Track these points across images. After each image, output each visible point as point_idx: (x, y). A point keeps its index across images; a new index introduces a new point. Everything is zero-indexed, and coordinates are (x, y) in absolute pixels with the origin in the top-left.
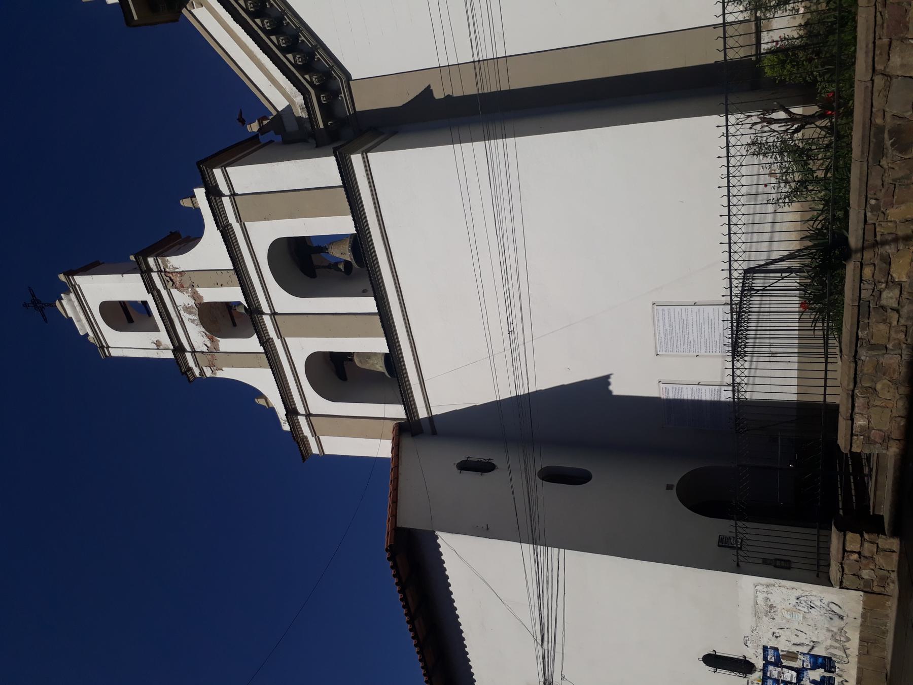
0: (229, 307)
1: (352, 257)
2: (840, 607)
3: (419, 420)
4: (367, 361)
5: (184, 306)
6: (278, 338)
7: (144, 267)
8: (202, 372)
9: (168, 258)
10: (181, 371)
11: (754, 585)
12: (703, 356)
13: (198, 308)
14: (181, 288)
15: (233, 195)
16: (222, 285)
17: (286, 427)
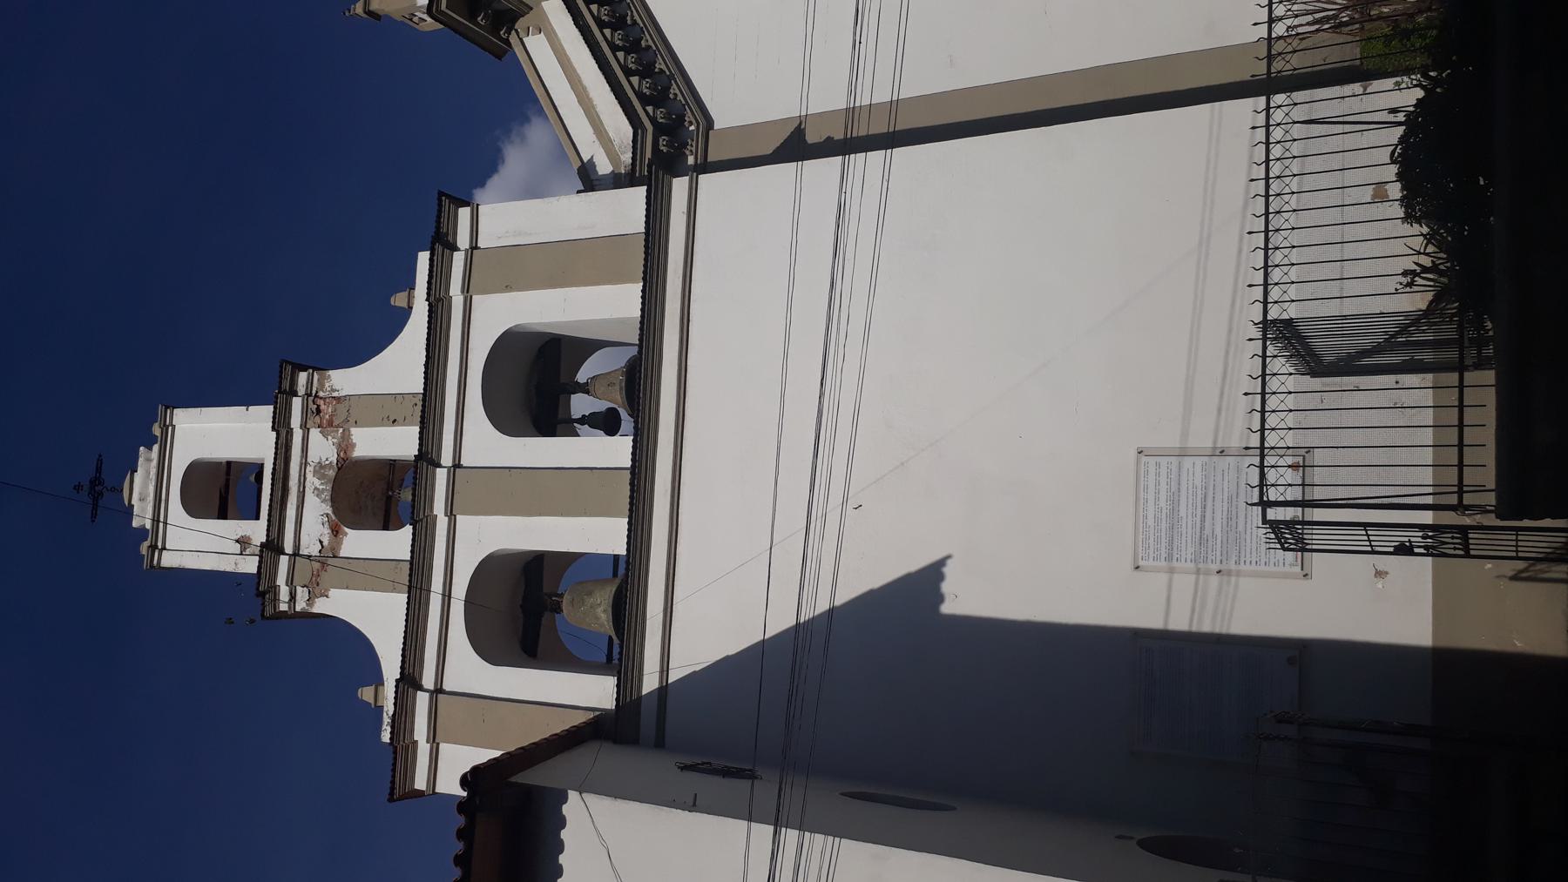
0: (391, 468)
1: (623, 384)
5: (319, 463)
6: (446, 515)
7: (286, 385)
8: (293, 597)
9: (331, 372)
10: (258, 589)
13: (339, 469)
14: (327, 427)
15: (474, 247)
16: (394, 421)
17: (386, 737)
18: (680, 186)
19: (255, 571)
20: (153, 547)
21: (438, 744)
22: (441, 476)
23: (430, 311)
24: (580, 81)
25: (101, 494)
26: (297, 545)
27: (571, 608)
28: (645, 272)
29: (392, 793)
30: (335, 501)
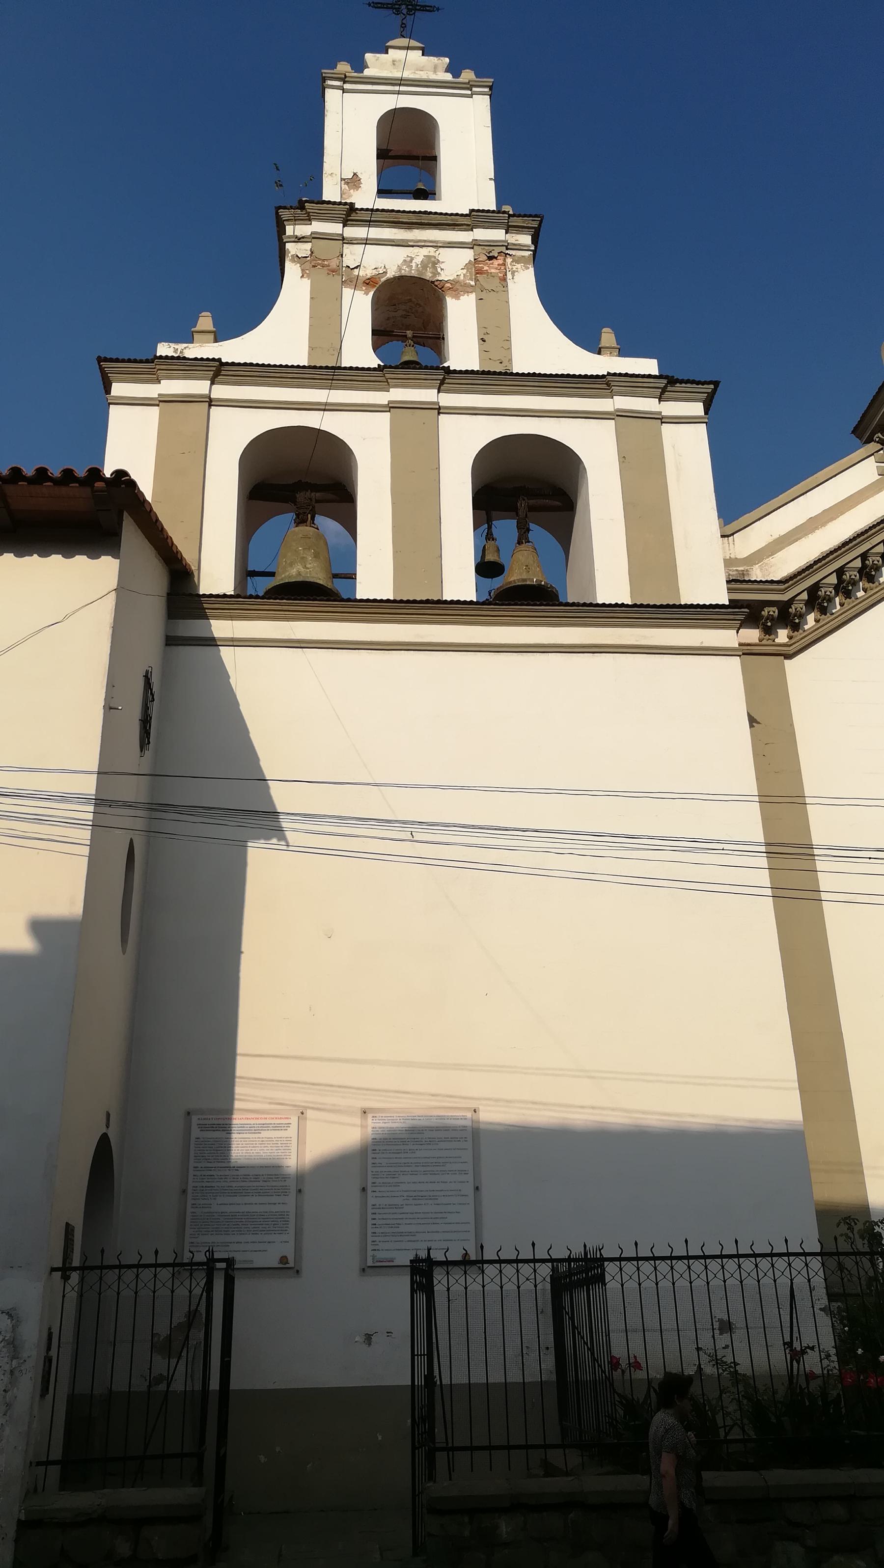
1: (528, 583)
3: (207, 618)
4: (309, 549)
6: (389, 402)
8: (299, 240)
9: (531, 270)
11: (14, 1309)
12: (364, 1204)
13: (433, 282)
14: (476, 269)
17: (164, 349)
18: (727, 637)
19: (325, 197)
20: (344, 80)
21: (158, 405)
22: (428, 395)
23: (597, 377)
24: (833, 519)
25: (398, 12)
26: (351, 242)
27: (301, 536)
28: (642, 606)
29: (106, 360)
30: (401, 281)
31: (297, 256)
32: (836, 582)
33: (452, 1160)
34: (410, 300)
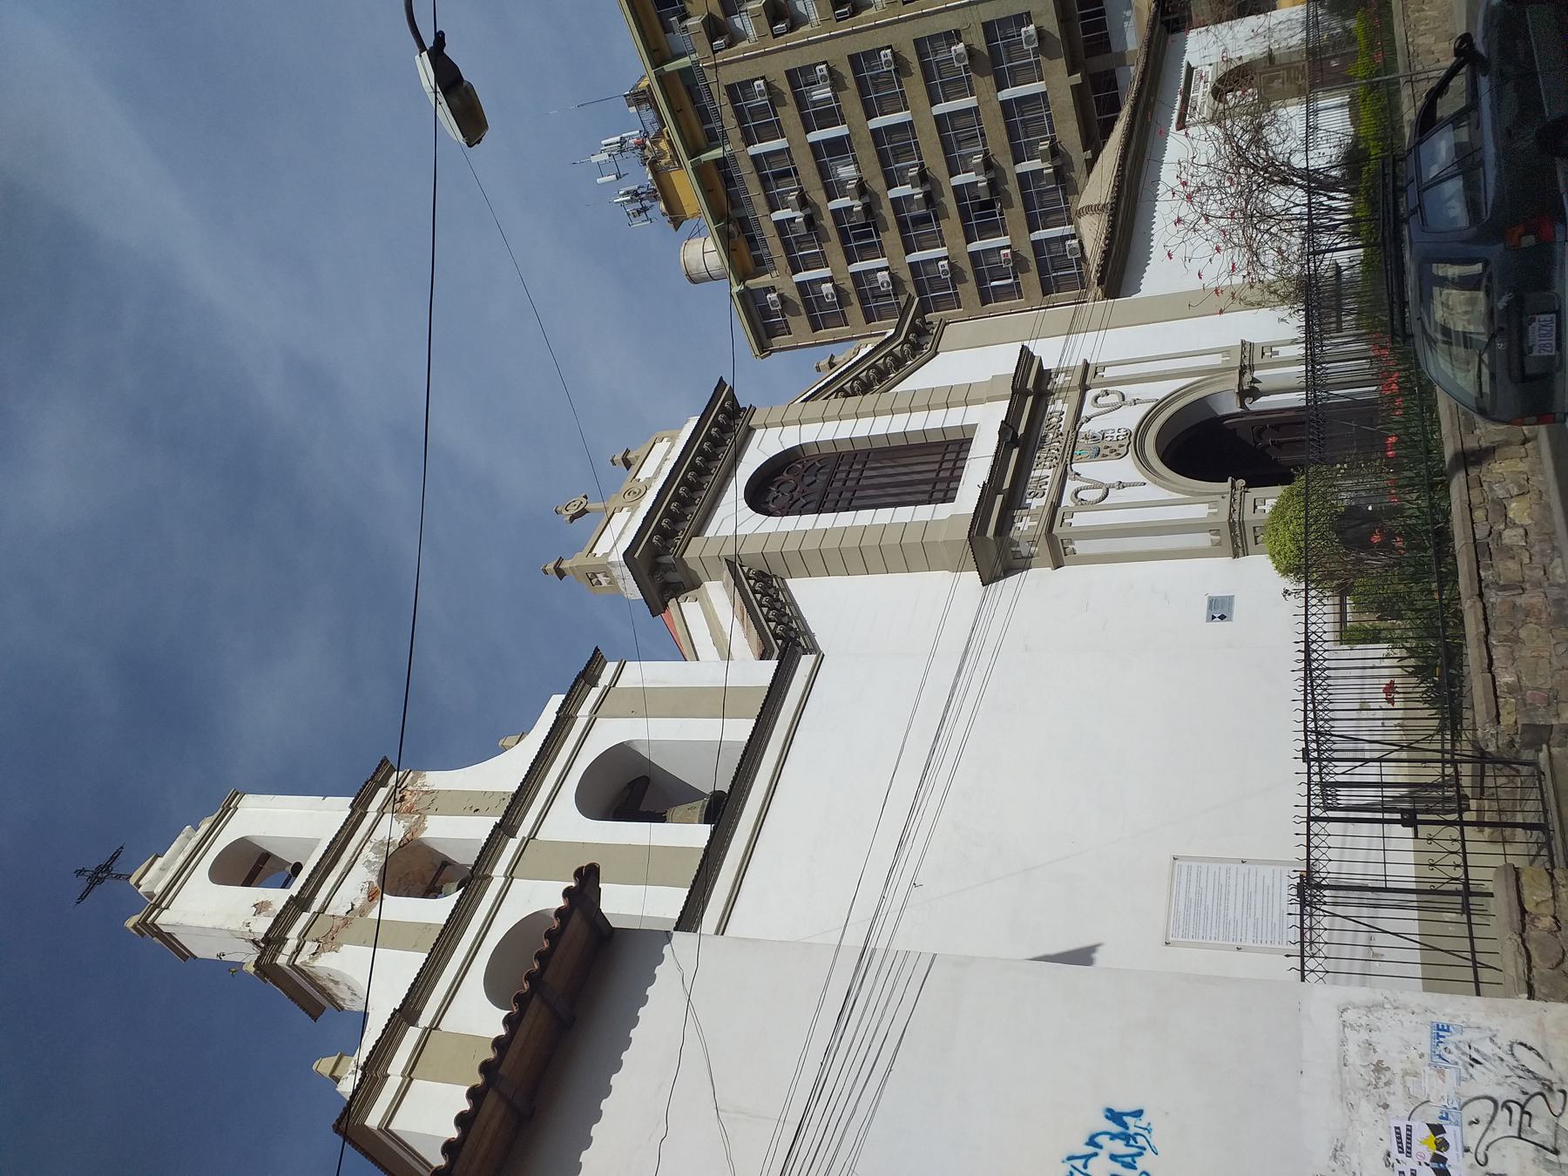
1: (706, 803)
2: (1539, 1055)
11: (1338, 1008)
13: (400, 847)
16: (477, 810)
18: (806, 662)
25: (101, 880)
29: (339, 1121)
31: (313, 954)
32: (774, 623)
33: (1217, 878)
34: (399, 881)
